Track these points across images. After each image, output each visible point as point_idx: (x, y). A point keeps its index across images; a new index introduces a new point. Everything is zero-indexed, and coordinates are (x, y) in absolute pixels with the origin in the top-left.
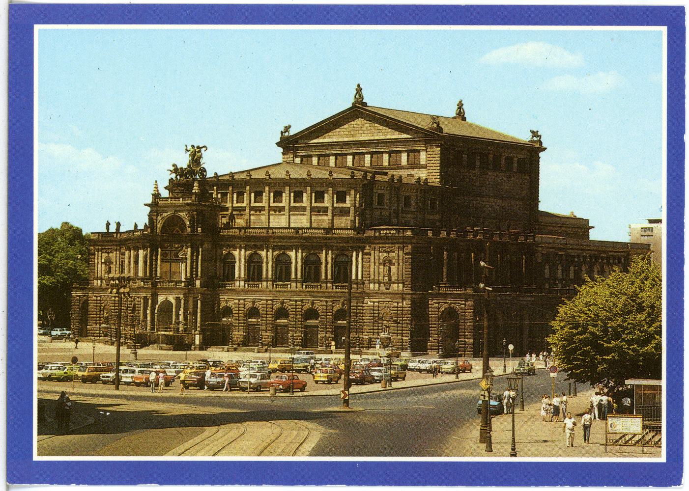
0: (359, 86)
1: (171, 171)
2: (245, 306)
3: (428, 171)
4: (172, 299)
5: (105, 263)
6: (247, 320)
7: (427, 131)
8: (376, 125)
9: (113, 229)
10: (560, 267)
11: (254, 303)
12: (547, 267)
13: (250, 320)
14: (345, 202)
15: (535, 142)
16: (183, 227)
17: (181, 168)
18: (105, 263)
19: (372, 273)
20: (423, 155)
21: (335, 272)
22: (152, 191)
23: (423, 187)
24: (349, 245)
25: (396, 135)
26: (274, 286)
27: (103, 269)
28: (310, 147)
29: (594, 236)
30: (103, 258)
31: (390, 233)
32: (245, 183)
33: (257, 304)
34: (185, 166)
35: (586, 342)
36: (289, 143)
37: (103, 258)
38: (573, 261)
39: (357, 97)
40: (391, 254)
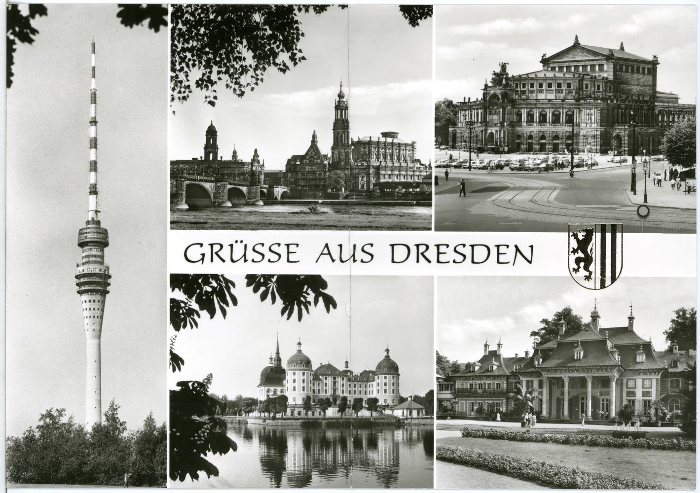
0: (576, 36)
4: (494, 132)
5: (464, 116)
9: (467, 100)
10: (666, 116)
12: (660, 116)
15: (655, 60)
16: (498, 99)
18: (464, 116)
20: (605, 67)
22: (484, 83)
23: (605, 80)
29: (681, 102)
32: (526, 79)
33: (532, 133)
34: (499, 72)
36: (545, 61)
38: (671, 113)
40: (592, 111)
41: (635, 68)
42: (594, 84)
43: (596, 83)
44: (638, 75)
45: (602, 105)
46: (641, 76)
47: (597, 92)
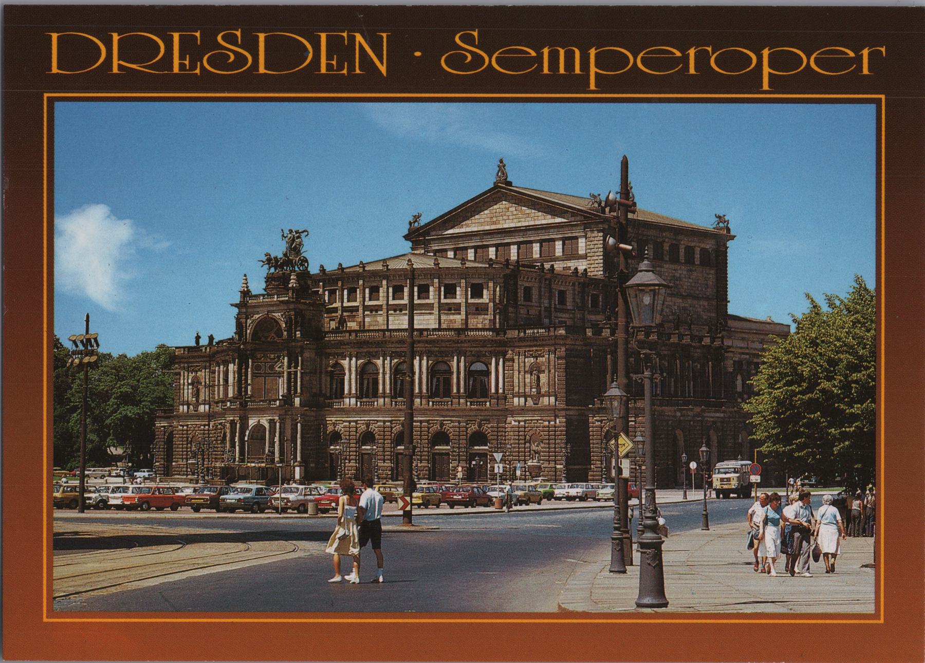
0: (501, 161)
1: (263, 262)
2: (357, 430)
3: (588, 262)
4: (265, 422)
5: (192, 384)
6: (359, 447)
7: (586, 212)
8: (523, 208)
9: (204, 341)
11: (368, 425)
13: (363, 447)
14: (481, 296)
15: (721, 229)
16: (279, 333)
17: (276, 258)
18: (192, 384)
19: (516, 383)
20: (582, 242)
21: (469, 386)
22: (239, 286)
23: (584, 281)
24: (486, 349)
25: (548, 220)
26: (393, 403)
27: (190, 391)
28: (444, 239)
30: (190, 377)
31: (538, 332)
32: (358, 276)
34: (280, 255)
35: (812, 406)
37: (190, 377)
39: (500, 174)
40: (540, 359)
41: (666, 247)
42: (550, 290)
43: (554, 286)
44: (676, 266)
45: (569, 342)
46: (682, 271)
47: (557, 310)
